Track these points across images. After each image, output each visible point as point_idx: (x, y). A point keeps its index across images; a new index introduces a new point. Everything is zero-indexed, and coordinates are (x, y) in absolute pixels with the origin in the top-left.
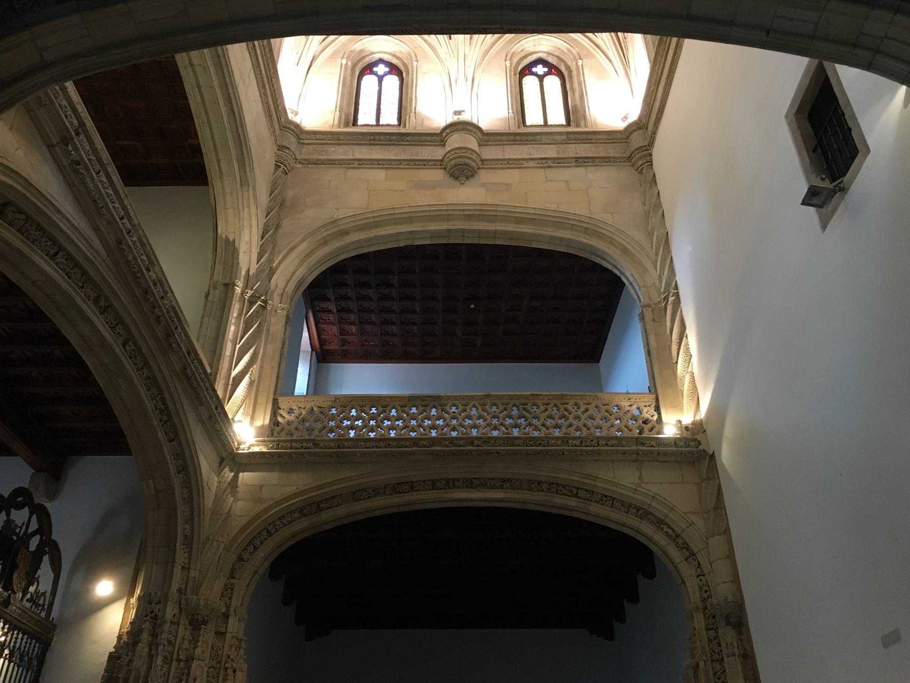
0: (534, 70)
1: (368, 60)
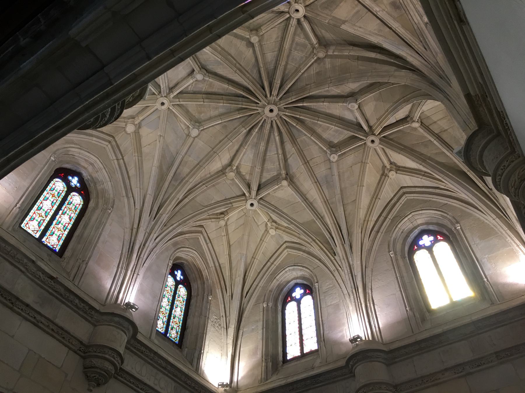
0: (421, 243)
1: (286, 290)
